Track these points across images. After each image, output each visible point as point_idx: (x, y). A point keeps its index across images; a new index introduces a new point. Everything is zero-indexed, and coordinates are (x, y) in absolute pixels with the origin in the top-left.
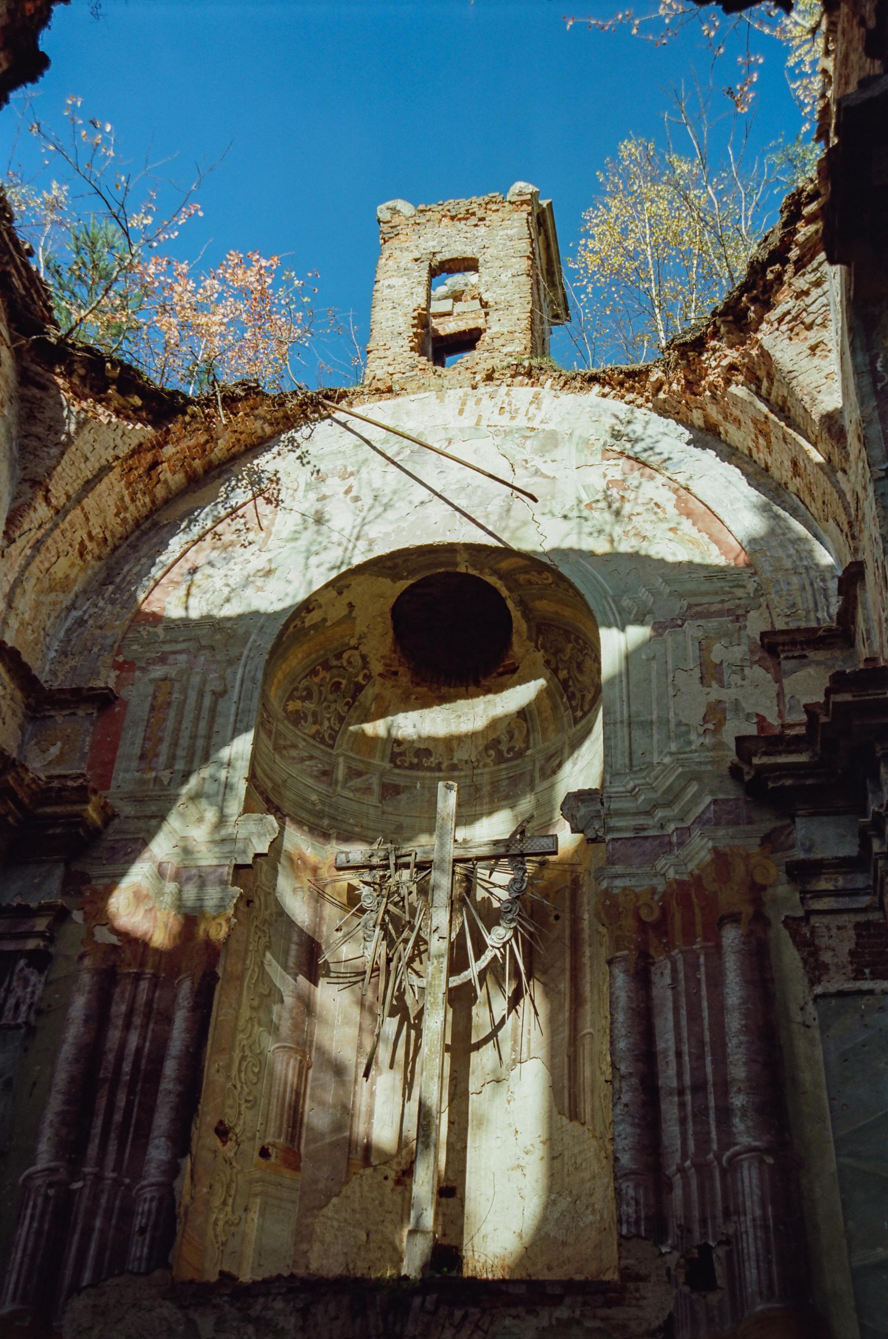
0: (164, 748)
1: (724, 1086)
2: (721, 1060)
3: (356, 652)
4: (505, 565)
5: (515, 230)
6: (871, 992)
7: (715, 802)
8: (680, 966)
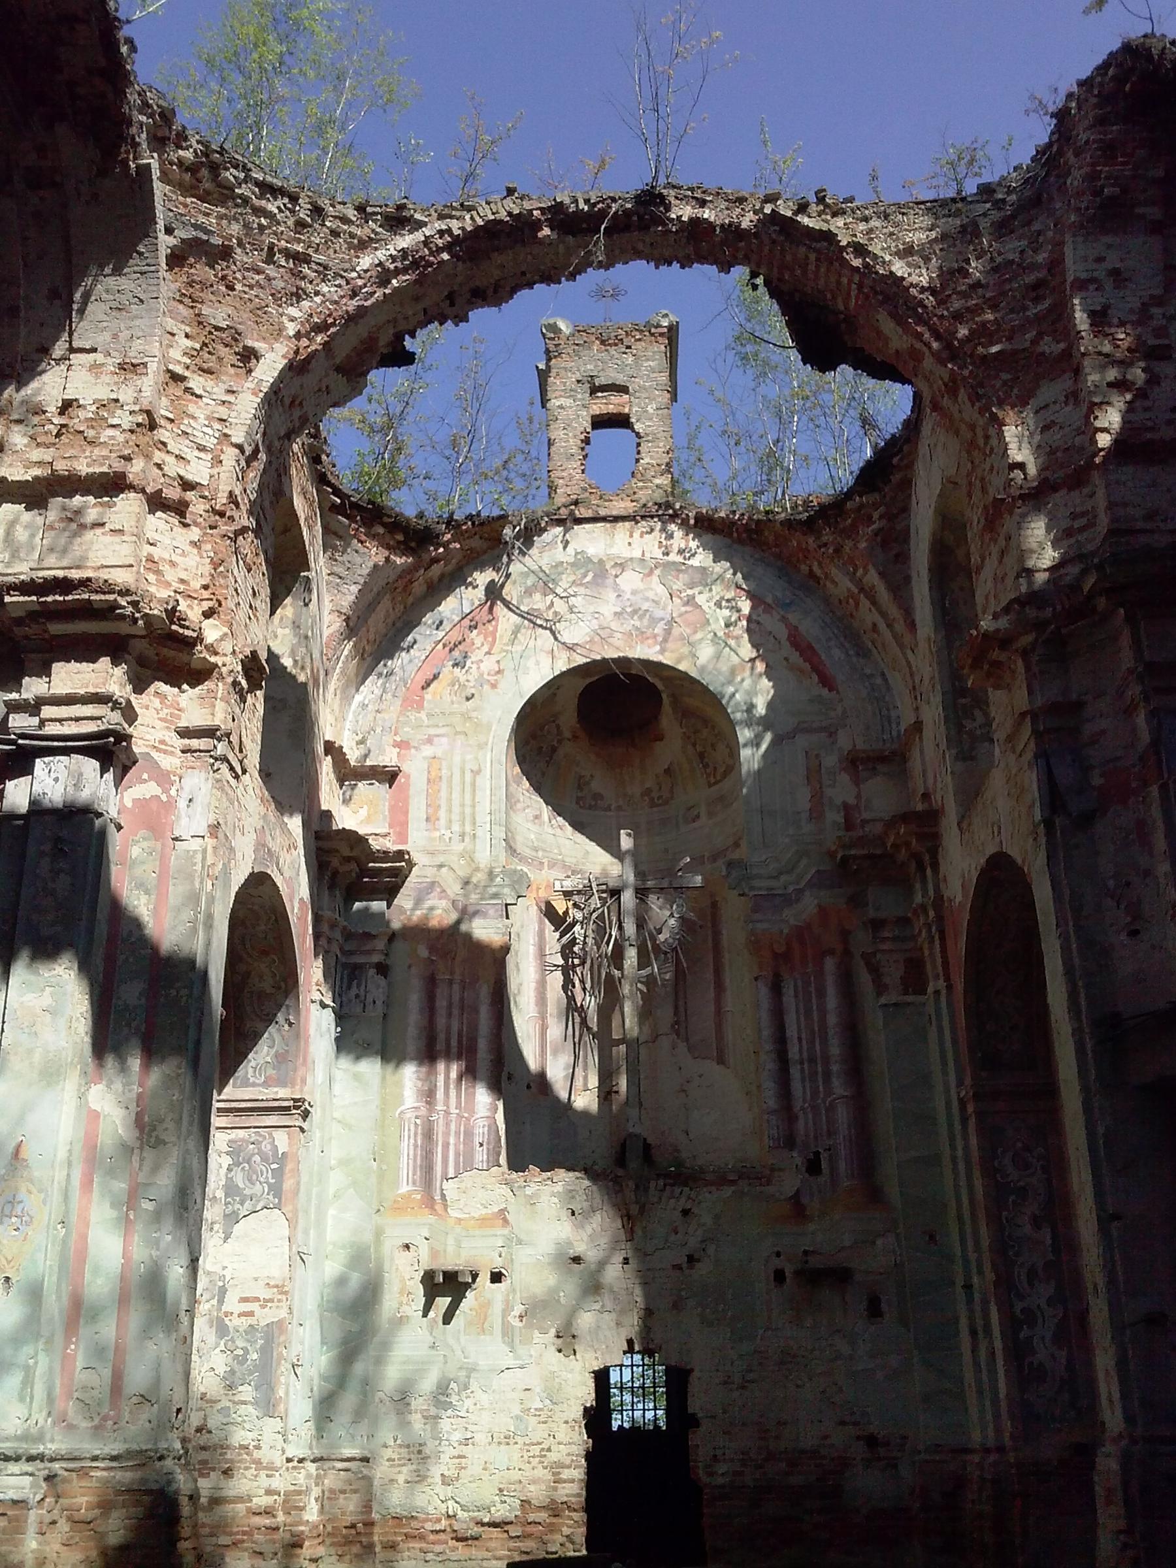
0: (442, 814)
1: (826, 1060)
2: (824, 1040)
4: (666, 673)
5: (656, 362)
6: (913, 1003)
7: (818, 871)
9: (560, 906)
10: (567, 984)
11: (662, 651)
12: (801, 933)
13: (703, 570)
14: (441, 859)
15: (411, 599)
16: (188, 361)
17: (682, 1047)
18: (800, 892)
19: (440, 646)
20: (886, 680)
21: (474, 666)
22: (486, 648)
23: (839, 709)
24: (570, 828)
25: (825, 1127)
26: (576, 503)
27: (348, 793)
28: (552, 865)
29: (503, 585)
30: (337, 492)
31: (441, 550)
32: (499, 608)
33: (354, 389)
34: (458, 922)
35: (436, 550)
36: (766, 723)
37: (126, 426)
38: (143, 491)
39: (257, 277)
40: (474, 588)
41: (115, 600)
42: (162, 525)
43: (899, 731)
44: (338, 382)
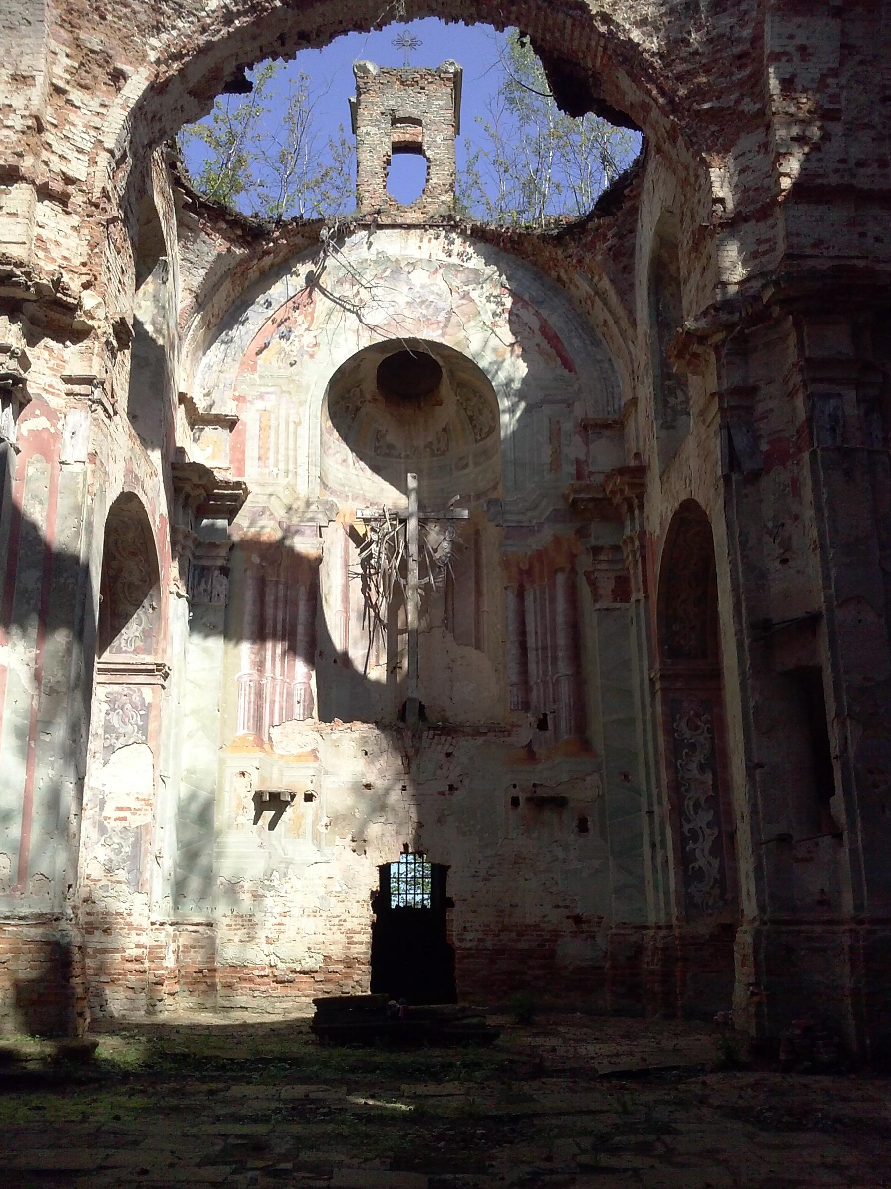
0: (271, 454)
1: (555, 647)
3: (358, 389)
4: (446, 352)
5: (444, 102)
8: (537, 592)
9: (361, 529)
10: (365, 588)
11: (443, 335)
12: (540, 555)
13: (476, 272)
14: (270, 490)
15: (247, 283)
16: (69, 77)
17: (449, 637)
18: (540, 525)
19: (270, 322)
20: (612, 365)
21: (297, 339)
22: (306, 326)
23: (576, 387)
24: (369, 471)
25: (552, 696)
26: (379, 212)
27: (197, 435)
28: (355, 498)
29: (320, 276)
30: (189, 193)
31: (272, 244)
32: (317, 294)
33: (203, 110)
34: (284, 538)
35: (267, 244)
36: (521, 395)
37: (19, 128)
38: (33, 183)
39: (124, 10)
40: (298, 276)
41: (12, 270)
42: (48, 212)
43: (620, 406)
44: (190, 102)
